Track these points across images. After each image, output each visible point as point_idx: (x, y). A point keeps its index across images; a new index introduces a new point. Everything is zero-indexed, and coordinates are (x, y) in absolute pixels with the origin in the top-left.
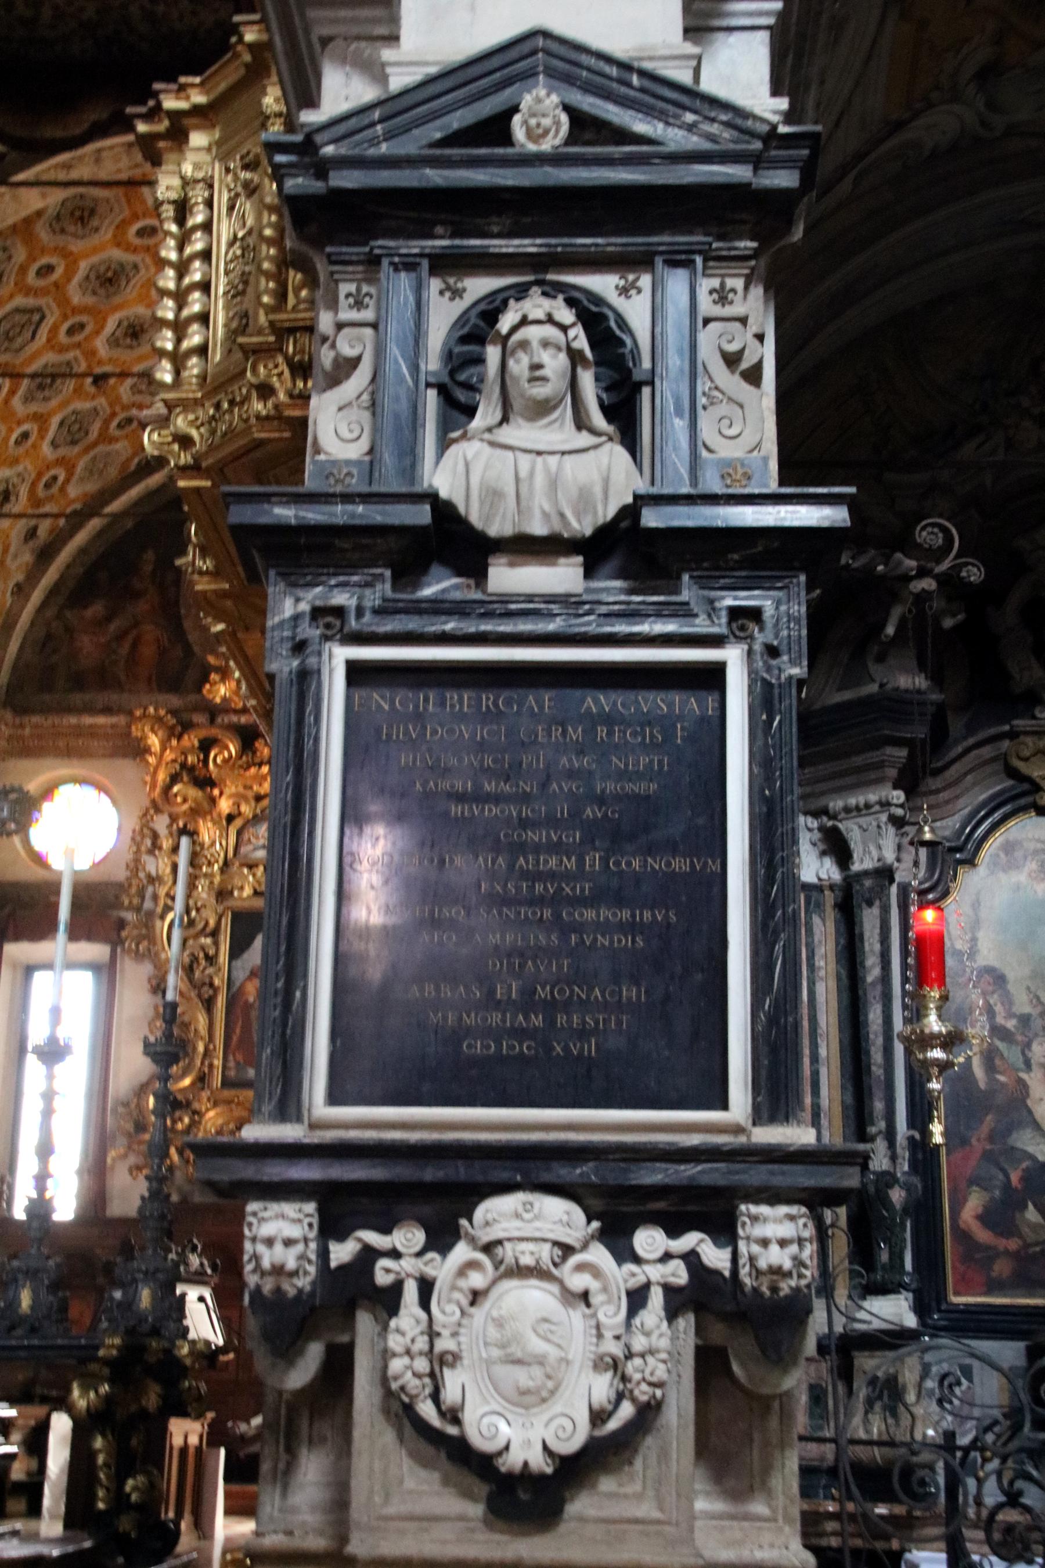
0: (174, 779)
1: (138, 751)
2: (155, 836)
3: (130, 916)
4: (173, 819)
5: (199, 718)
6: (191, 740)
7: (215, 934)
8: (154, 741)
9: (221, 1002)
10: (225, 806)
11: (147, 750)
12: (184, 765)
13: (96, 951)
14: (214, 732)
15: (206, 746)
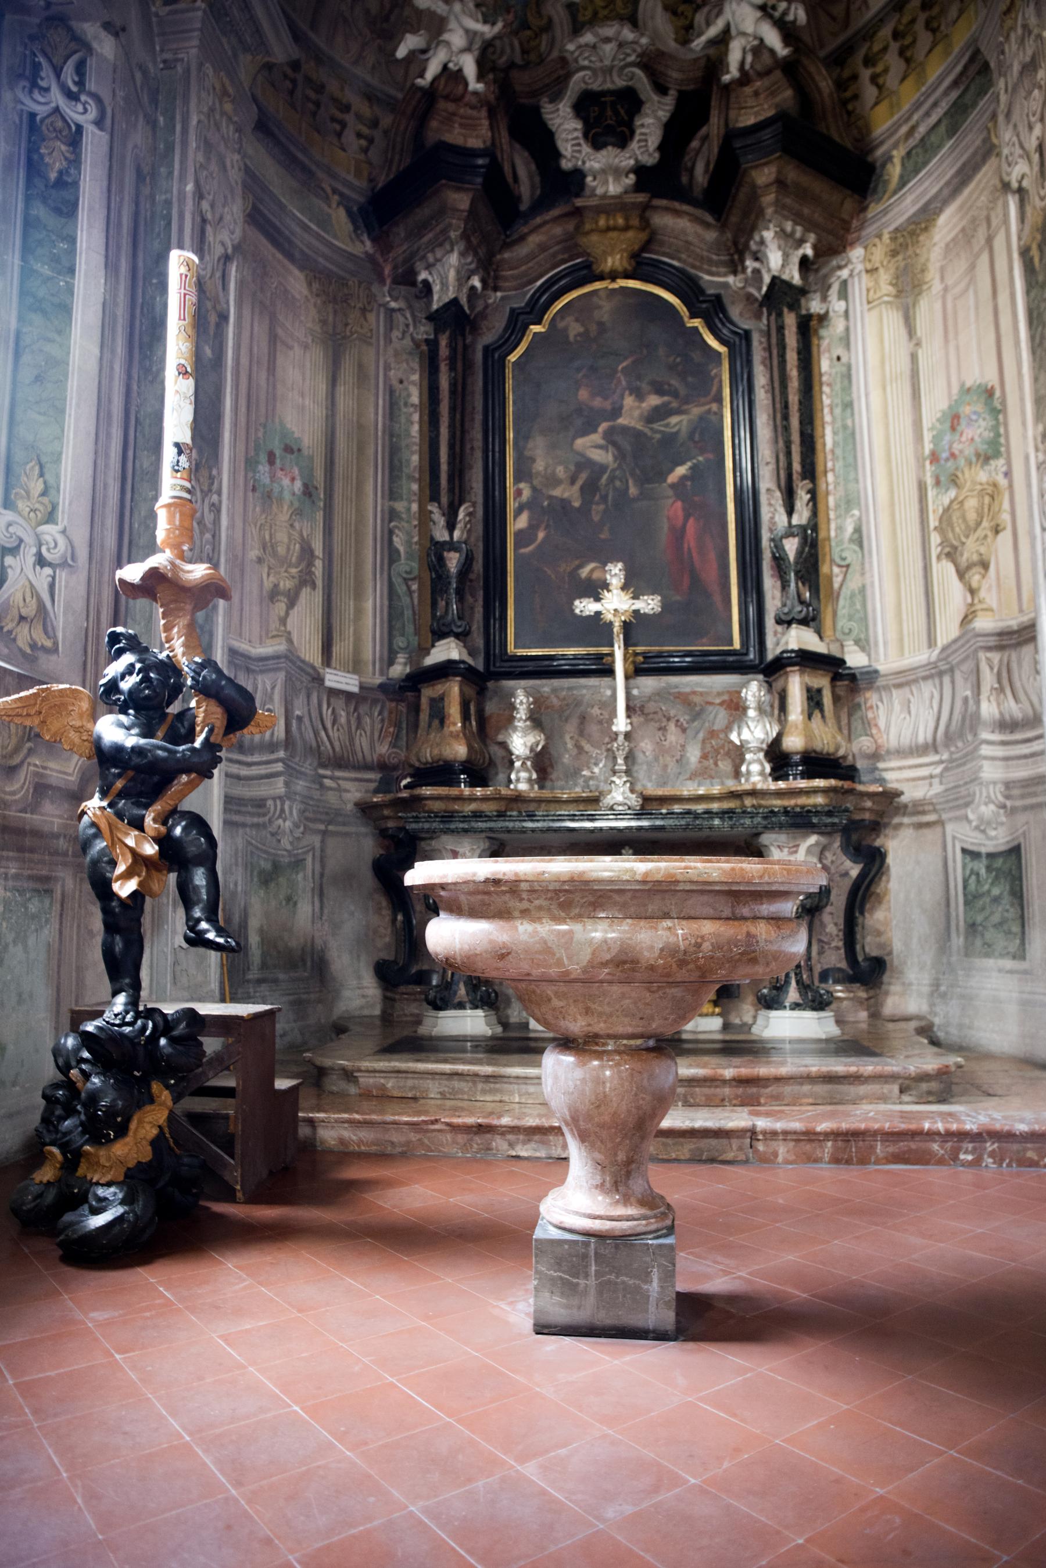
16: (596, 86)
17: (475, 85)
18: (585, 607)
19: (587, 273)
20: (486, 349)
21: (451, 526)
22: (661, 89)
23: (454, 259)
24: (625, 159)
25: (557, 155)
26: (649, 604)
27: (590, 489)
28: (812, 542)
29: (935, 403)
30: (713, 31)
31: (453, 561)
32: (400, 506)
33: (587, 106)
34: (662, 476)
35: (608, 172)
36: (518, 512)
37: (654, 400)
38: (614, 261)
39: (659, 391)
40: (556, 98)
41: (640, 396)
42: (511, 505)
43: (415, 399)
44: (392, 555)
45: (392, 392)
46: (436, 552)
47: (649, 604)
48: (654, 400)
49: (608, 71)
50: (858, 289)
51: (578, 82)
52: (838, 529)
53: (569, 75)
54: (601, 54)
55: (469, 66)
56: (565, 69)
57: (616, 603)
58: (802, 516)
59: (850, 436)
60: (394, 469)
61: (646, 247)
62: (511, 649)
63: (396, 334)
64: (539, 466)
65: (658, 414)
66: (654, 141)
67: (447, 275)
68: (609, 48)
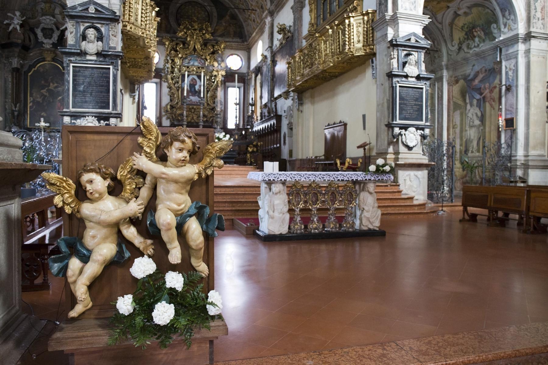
0: (171, 50)
1: (164, 44)
2: (168, 60)
3: (163, 74)
4: (170, 57)
5: (174, 39)
6: (174, 43)
7: (179, 78)
8: (167, 43)
9: (180, 90)
10: (180, 55)
11: (165, 44)
12: (173, 48)
13: (157, 80)
14: (178, 42)
15: (177, 44)
16: (46, 27)
17: (19, 31)
18: (37, 124)
19: (44, 60)
20: (24, 72)
21: (16, 107)
22: (58, 29)
23: (16, 59)
24: (51, 42)
25: (38, 38)
27: (43, 99)
30: (63, 27)
31: (16, 113)
32: (7, 100)
33: (43, 30)
34: (57, 98)
36: (30, 103)
37: (56, 85)
38: (49, 59)
39: (57, 83)
40: (37, 28)
41: (53, 84)
42: (29, 101)
43: (10, 80)
44: (6, 109)
45: (5, 79)
46: (13, 112)
48: (56, 85)
49: (48, 24)
53: (41, 23)
54: (47, 21)
56: (40, 23)
57: (43, 124)
60: (6, 93)
61: (55, 56)
62: (28, 126)
63: (6, 68)
64: (34, 95)
65: (56, 87)
66: (56, 39)
68: (48, 20)
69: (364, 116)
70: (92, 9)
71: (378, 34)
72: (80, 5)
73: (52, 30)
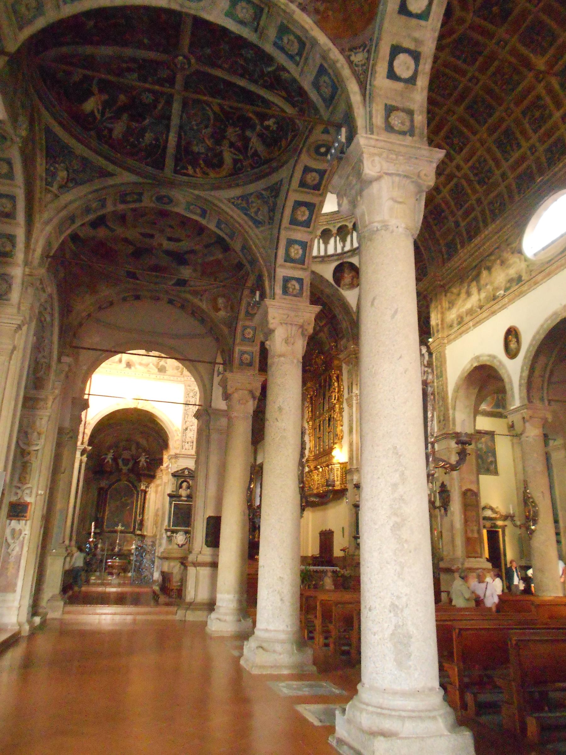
19: (120, 480)
24: (127, 468)
26: (123, 528)
28: (142, 521)
29: (156, 508)
33: (123, 460)
35: (125, 469)
47: (123, 528)
50: (152, 488)
51: (123, 457)
52: (146, 517)
54: (126, 455)
55: (110, 461)
58: (141, 518)
59: (149, 506)
67: (104, 484)
69: (343, 528)
70: (186, 472)
71: (349, 477)
72: (181, 470)
73: (128, 460)
